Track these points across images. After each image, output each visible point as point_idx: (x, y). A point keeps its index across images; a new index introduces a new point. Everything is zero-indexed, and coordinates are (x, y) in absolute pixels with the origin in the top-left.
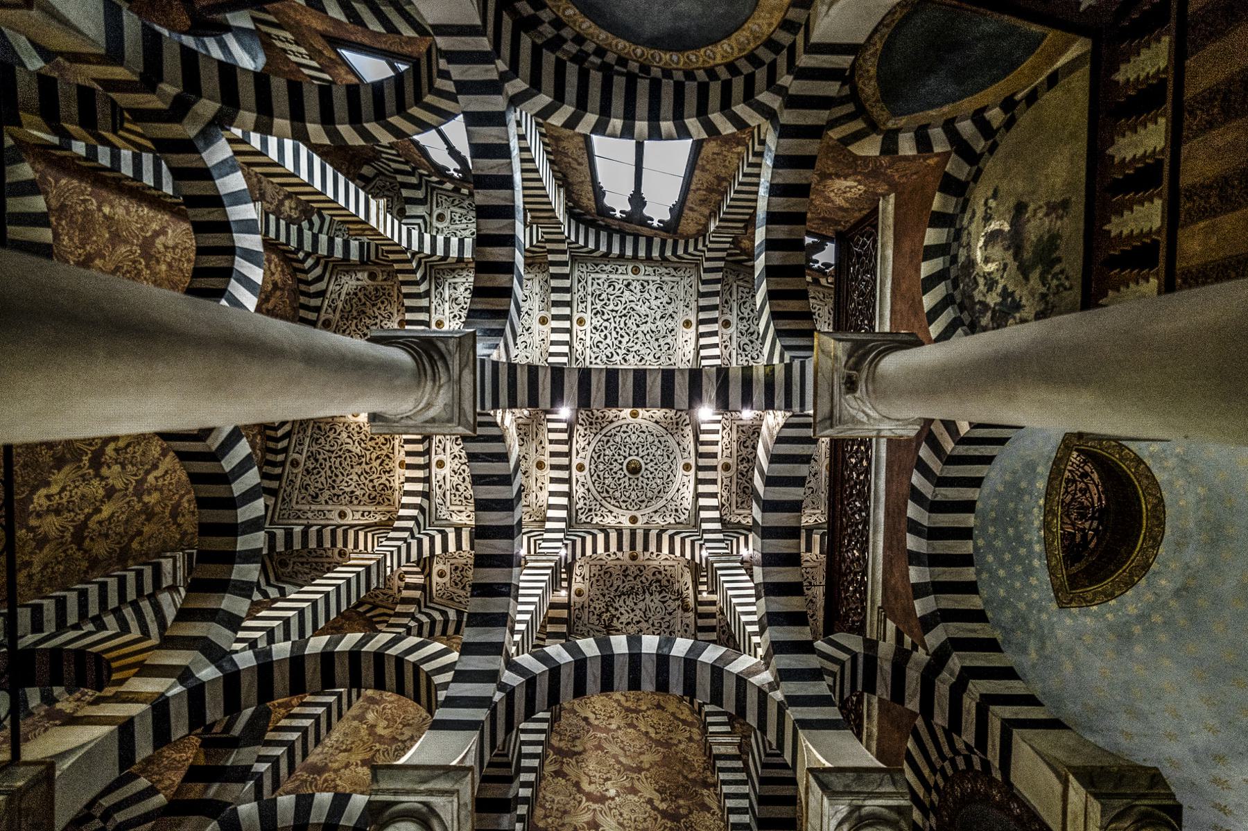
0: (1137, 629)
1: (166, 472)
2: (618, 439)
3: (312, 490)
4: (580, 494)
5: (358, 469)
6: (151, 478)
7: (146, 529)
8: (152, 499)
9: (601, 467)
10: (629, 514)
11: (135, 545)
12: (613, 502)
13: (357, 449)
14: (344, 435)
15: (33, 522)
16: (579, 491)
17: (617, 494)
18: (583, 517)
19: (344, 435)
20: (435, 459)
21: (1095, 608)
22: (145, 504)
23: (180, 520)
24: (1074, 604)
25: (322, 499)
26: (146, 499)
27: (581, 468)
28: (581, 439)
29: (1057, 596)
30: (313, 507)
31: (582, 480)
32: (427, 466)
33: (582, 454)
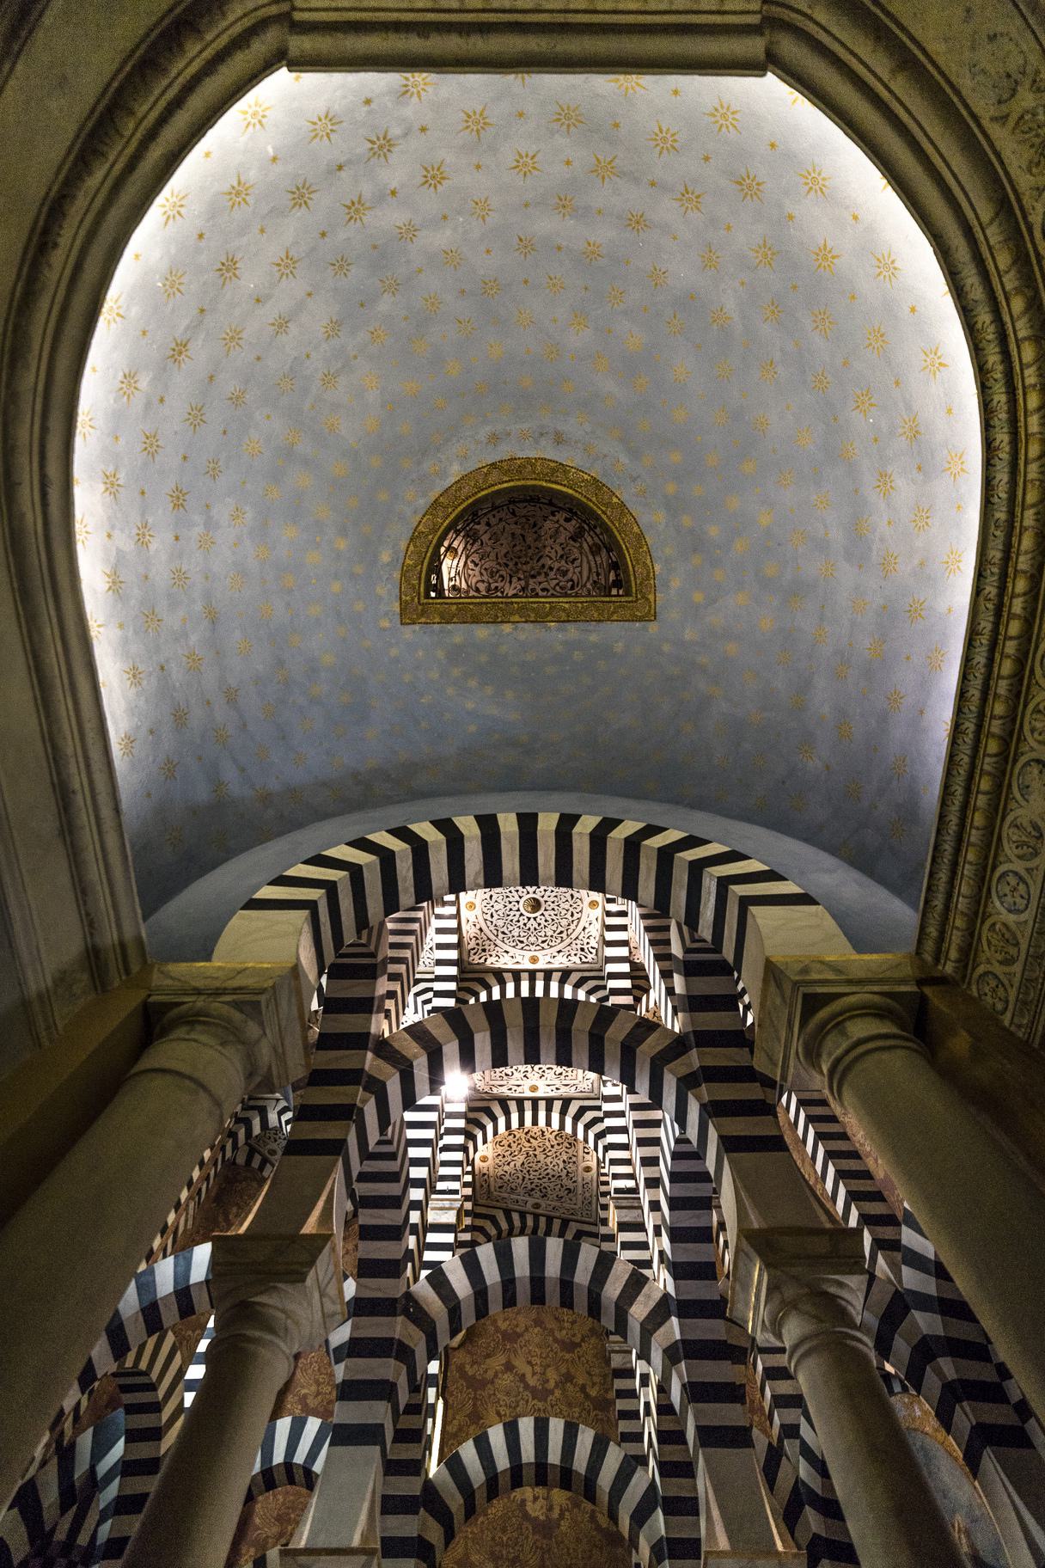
0: (686, 521)
1: (529, 1363)
2: (500, 923)
3: (563, 1193)
4: (565, 960)
5: (541, 1157)
6: (532, 1381)
7: (581, 1382)
8: (553, 1376)
9: (532, 939)
10: (587, 910)
11: (593, 1393)
12: (572, 927)
13: (521, 1158)
14: (506, 1168)
15: (556, 1514)
16: (560, 962)
17: (564, 923)
18: (590, 957)
19: (506, 1168)
20: (528, 1094)
21: (657, 568)
22: (557, 1386)
23: (577, 1340)
24: (651, 597)
25: (571, 1186)
26: (552, 1384)
27: (534, 960)
28: (502, 960)
29: (640, 620)
30: (580, 1190)
31: (548, 959)
32: (535, 1101)
33: (519, 959)
